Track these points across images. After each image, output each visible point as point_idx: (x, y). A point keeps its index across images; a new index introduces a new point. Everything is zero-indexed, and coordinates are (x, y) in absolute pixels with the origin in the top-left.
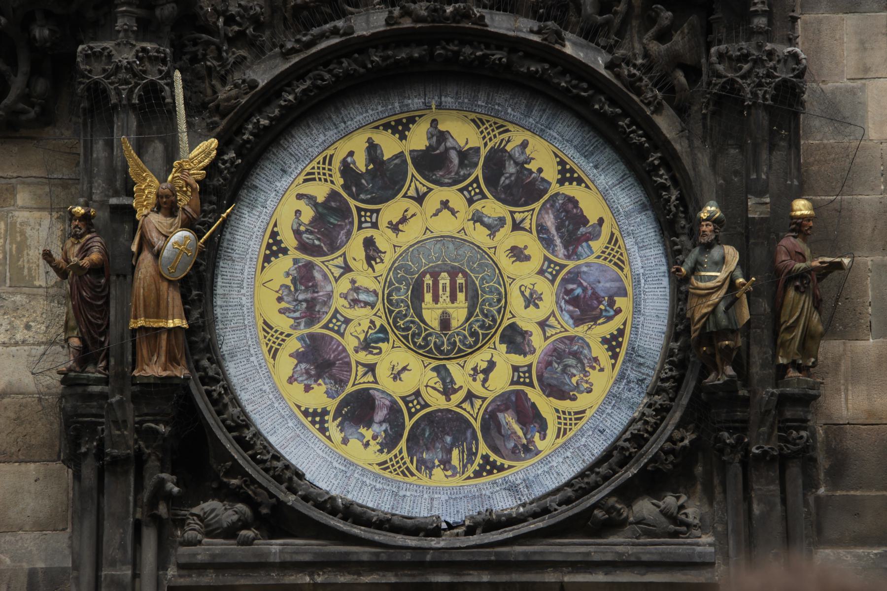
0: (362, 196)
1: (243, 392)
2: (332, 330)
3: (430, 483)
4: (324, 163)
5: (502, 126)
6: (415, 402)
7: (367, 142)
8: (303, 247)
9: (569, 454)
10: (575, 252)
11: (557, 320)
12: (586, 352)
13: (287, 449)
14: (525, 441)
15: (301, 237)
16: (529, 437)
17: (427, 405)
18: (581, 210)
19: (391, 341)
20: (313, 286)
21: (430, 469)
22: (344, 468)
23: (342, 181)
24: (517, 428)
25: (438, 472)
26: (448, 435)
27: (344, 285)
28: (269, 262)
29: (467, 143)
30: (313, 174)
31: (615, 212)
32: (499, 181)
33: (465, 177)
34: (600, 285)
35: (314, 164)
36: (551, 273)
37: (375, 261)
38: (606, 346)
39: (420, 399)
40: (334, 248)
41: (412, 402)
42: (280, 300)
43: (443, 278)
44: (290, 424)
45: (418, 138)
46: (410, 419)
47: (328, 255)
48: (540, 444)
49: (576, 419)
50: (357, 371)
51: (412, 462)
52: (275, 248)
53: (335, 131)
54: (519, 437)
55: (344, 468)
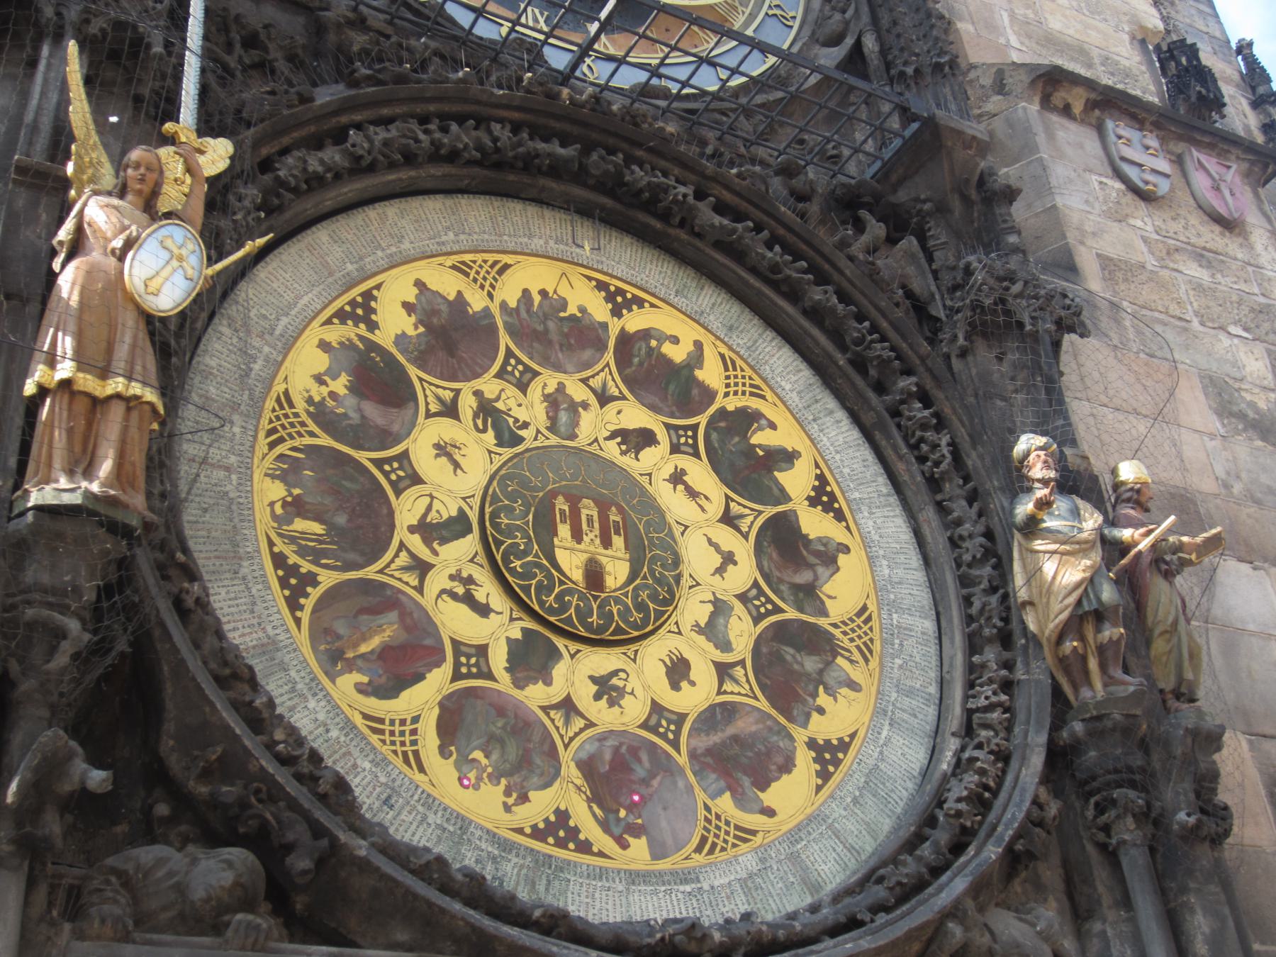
3: (257, 476)
5: (871, 652)
7: (794, 451)
8: (625, 340)
9: (334, 733)
12: (535, 780)
13: (307, 253)
14: (350, 655)
15: (640, 339)
16: (359, 662)
17: (398, 493)
18: (778, 779)
20: (570, 345)
21: (283, 477)
22: (277, 332)
23: (730, 408)
24: (375, 643)
25: (277, 491)
26: (349, 521)
27: (577, 392)
29: (830, 597)
31: (795, 835)
32: (787, 645)
35: (748, 372)
42: (543, 293)
44: (350, 267)
45: (814, 524)
48: (348, 681)
49: (405, 754)
51: (294, 449)
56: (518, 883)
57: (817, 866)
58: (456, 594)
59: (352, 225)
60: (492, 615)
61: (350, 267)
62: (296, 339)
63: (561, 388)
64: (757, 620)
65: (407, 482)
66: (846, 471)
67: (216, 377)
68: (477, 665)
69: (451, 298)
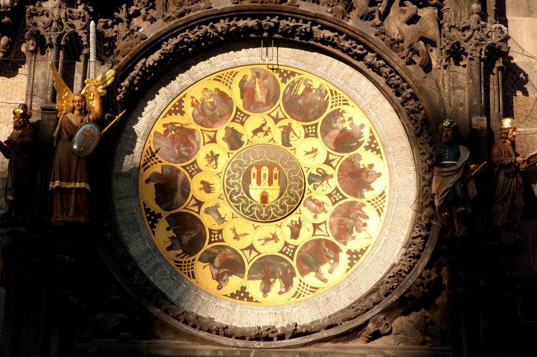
2: (341, 194)
4: (300, 294)
6: (310, 131)
8: (337, 250)
9: (236, 60)
11: (204, 139)
13: (399, 135)
16: (253, 81)
17: (304, 127)
18: (156, 194)
19: (308, 173)
21: (319, 89)
22: (370, 110)
23: (294, 279)
24: (258, 89)
27: (322, 217)
28: (362, 250)
32: (196, 235)
37: (296, 224)
38: (183, 109)
39: (307, 132)
40: (319, 241)
41: (312, 132)
42: (365, 225)
43: (265, 170)
44: (391, 149)
45: (234, 283)
46: (317, 123)
47: (324, 239)
49: (221, 77)
50: (337, 164)
52: (355, 256)
53: (284, 310)
54: (259, 83)
57: (123, 182)
59: (408, 158)
60: (253, 135)
61: (391, 149)
62: (366, 116)
63: (325, 211)
64: (210, 230)
65: (307, 132)
66: (249, 312)
69: (372, 185)
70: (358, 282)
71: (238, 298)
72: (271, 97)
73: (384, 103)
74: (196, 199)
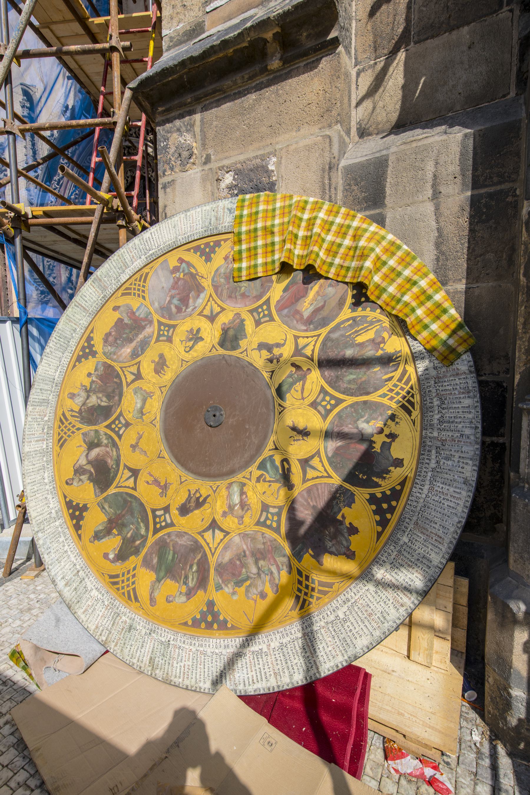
0: (143, 531)
1: (388, 618)
5: (61, 420)
8: (202, 582)
10: (145, 319)
12: (222, 270)
13: (440, 533)
15: (193, 588)
17: (323, 390)
19: (271, 453)
20: (239, 559)
22: (434, 452)
23: (133, 558)
28: (225, 622)
29: (81, 446)
30: (129, 592)
33: (110, 437)
34: (165, 285)
36: (168, 331)
40: (196, 547)
41: (325, 407)
44: (405, 539)
45: (86, 492)
46: (343, 401)
47: (205, 551)
50: (313, 478)
53: (86, 580)
55: (434, 452)
56: (223, 216)
58: (277, 347)
60: (256, 347)
61: (405, 539)
62: (420, 454)
65: (318, 400)
66: (62, 539)
67: (459, 393)
68: (259, 314)
70: (178, 655)
71: (71, 511)
72: (319, 316)
73: (470, 462)
74: (139, 368)
